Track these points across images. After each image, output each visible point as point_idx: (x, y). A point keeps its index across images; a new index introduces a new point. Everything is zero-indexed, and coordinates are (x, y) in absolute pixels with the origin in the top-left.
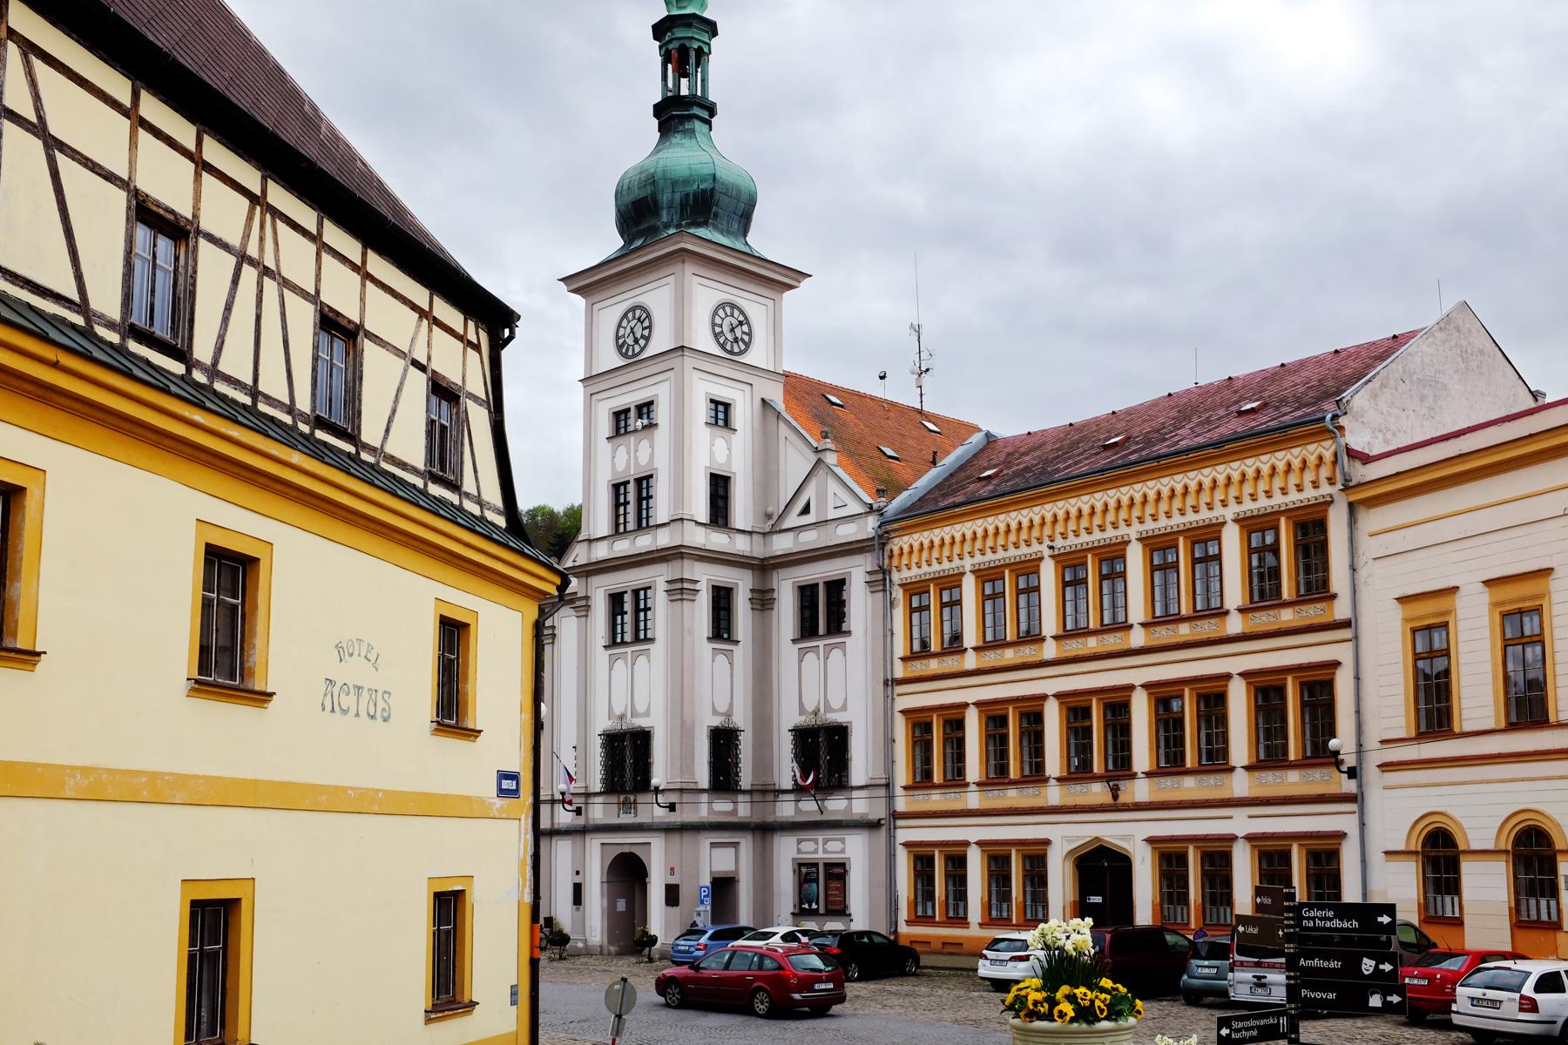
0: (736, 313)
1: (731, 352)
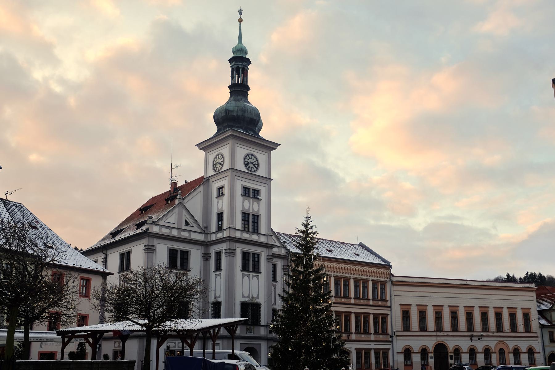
0: (253, 157)
1: (251, 171)
